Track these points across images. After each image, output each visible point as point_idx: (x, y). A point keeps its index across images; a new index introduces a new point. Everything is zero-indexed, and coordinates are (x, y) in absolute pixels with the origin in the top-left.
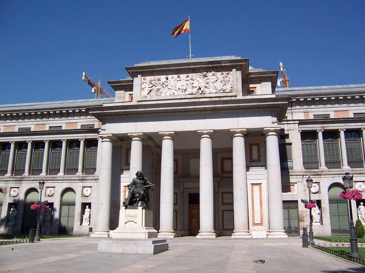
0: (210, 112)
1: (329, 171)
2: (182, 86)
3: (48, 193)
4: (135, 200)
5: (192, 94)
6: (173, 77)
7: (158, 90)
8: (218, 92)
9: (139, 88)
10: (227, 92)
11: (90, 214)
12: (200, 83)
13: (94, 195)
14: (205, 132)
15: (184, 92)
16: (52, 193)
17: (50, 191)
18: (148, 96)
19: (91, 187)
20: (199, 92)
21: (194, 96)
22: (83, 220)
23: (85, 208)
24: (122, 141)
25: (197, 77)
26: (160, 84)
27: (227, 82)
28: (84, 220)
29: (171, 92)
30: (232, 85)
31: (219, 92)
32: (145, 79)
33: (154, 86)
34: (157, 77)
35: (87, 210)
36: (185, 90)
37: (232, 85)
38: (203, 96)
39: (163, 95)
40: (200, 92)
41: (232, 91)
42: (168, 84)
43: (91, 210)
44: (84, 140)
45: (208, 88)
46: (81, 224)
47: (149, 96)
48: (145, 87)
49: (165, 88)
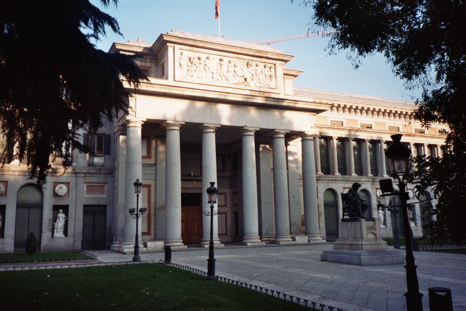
1: (325, 177)
2: (226, 73)
10: (271, 88)
11: (66, 222)
13: (72, 194)
14: (252, 129)
15: (228, 80)
19: (69, 183)
20: (244, 83)
21: (239, 87)
23: (59, 212)
25: (241, 64)
30: (276, 81)
33: (195, 65)
34: (199, 55)
35: (61, 216)
37: (276, 81)
40: (246, 84)
41: (276, 88)
45: (252, 80)
46: (53, 236)
49: (208, 70)
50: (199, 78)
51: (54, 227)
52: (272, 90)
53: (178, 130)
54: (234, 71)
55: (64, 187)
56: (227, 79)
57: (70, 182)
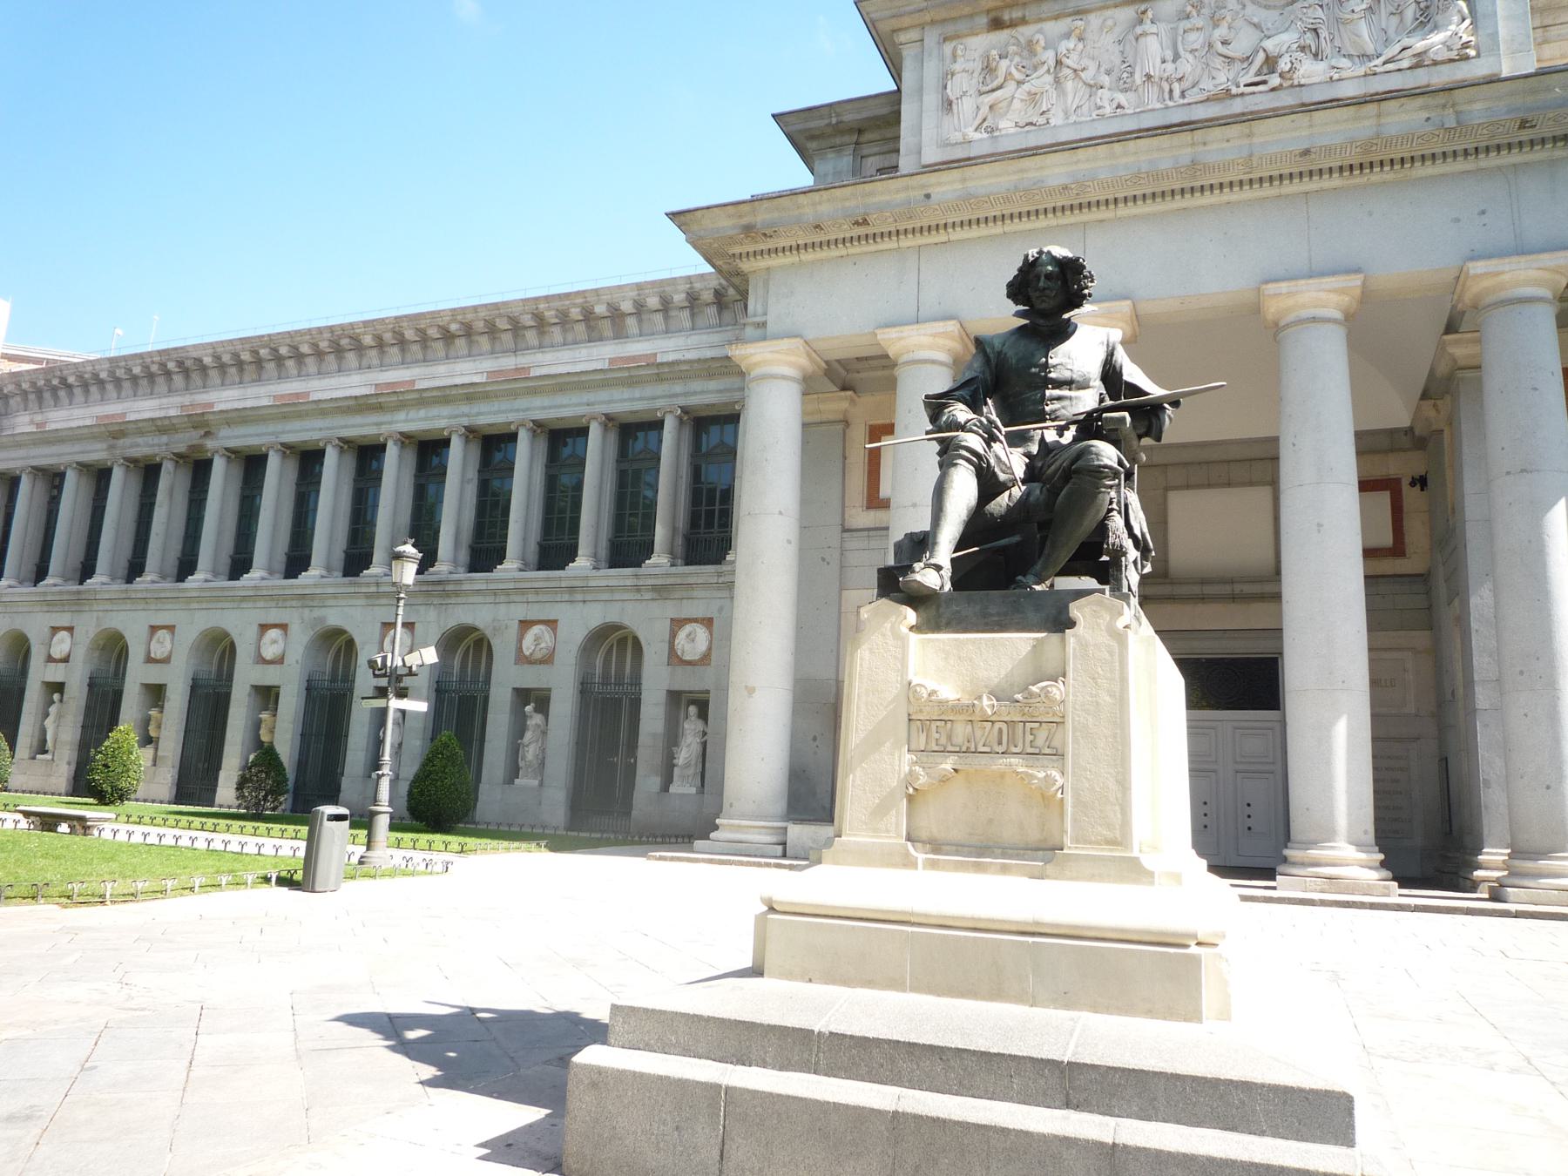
0: (1336, 181)
3: (528, 649)
4: (1016, 539)
5: (1228, 95)
6: (1110, 23)
7: (1033, 98)
8: (1378, 70)
9: (931, 99)
11: (704, 745)
12: (1266, 32)
15: (1177, 93)
16: (543, 645)
17: (537, 639)
18: (977, 136)
19: (712, 619)
20: (1264, 82)
21: (1237, 106)
22: (676, 769)
24: (849, 393)
26: (1045, 67)
27: (1433, 10)
28: (676, 771)
29: (1106, 104)
30: (1468, 22)
31: (1390, 67)
32: (959, 52)
34: (1024, 32)
35: (691, 727)
36: (1180, 79)
37: (1468, 22)
38: (1286, 99)
39: (1057, 119)
40: (1275, 80)
41: (1472, 53)
42: (1085, 62)
43: (707, 723)
44: (679, 411)
45: (1316, 55)
47: (985, 135)
48: (965, 93)
49: (1069, 85)
50: (1027, 128)
51: (675, 761)
52: (1444, 68)
53: (941, 364)
54: (1210, 46)
55: (701, 634)
56: (1171, 91)
57: (715, 615)
